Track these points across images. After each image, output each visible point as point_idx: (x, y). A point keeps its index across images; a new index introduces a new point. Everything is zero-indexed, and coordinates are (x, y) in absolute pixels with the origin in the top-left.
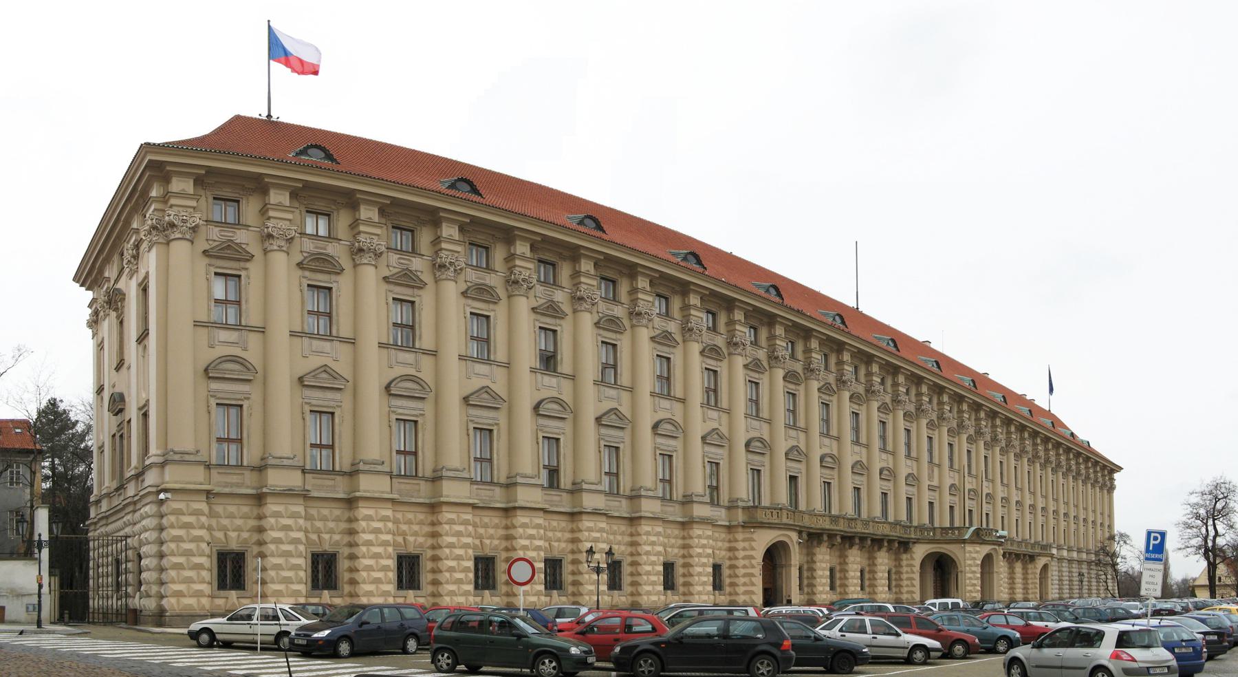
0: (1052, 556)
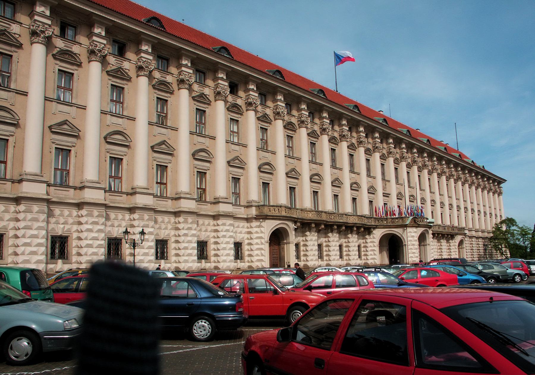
0: (465, 234)
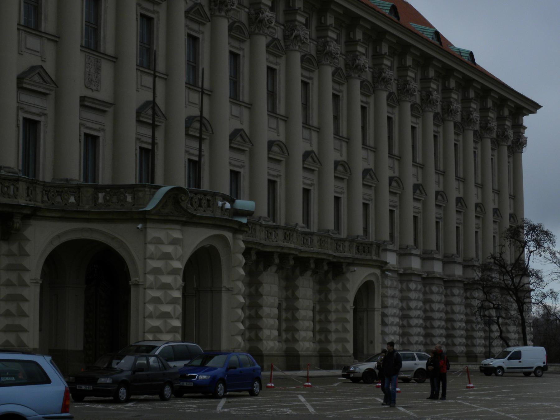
0: (382, 266)
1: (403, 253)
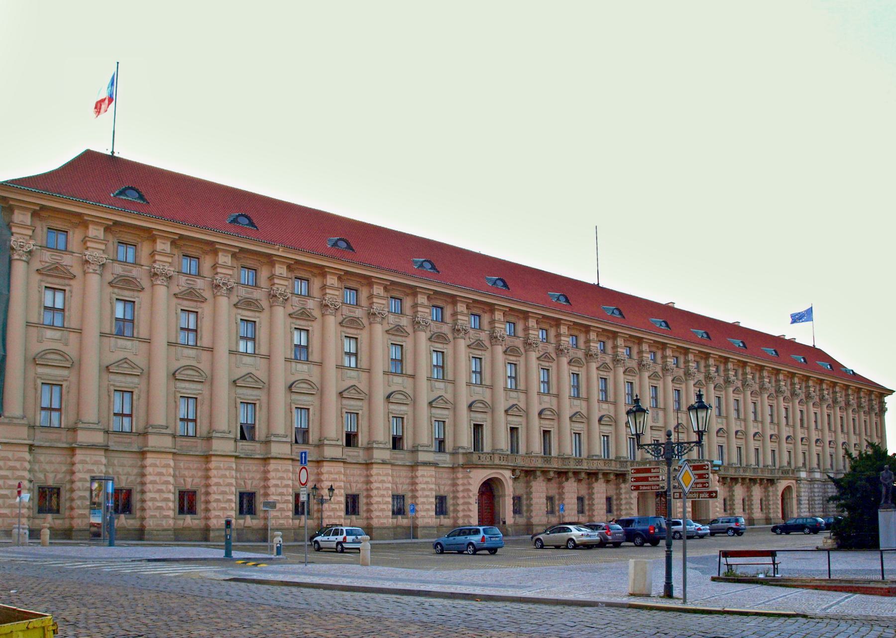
1: (811, 471)
